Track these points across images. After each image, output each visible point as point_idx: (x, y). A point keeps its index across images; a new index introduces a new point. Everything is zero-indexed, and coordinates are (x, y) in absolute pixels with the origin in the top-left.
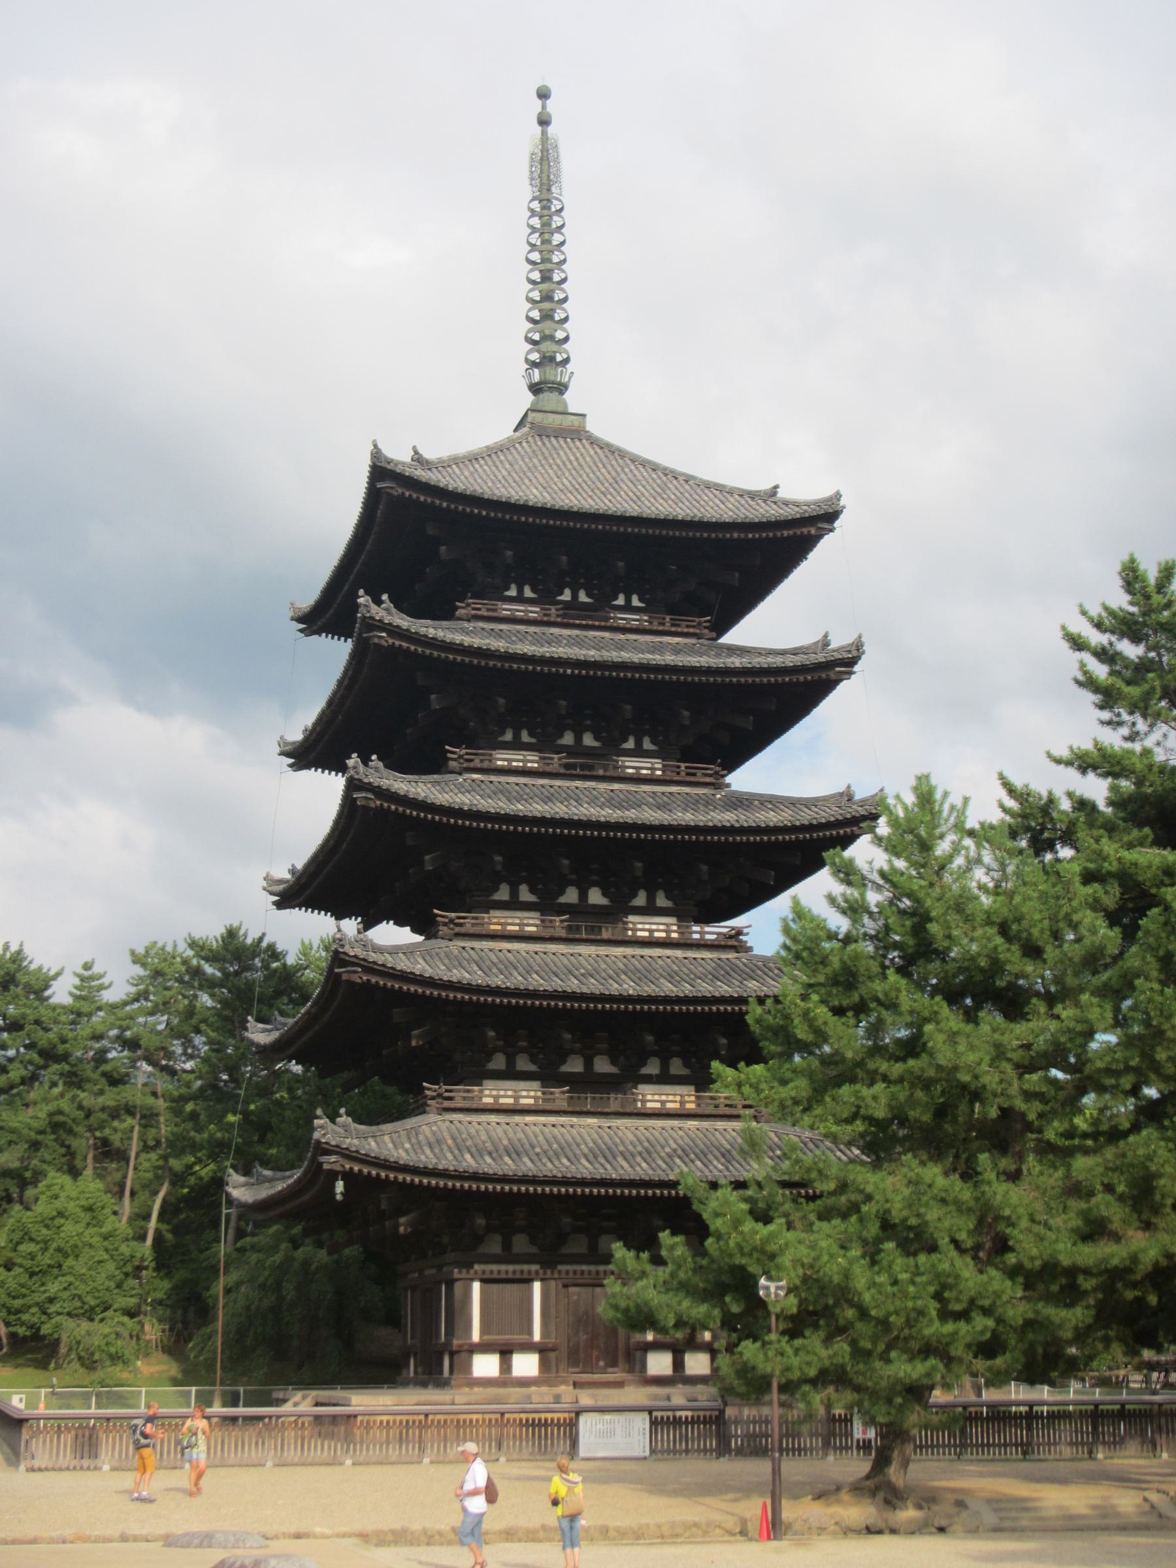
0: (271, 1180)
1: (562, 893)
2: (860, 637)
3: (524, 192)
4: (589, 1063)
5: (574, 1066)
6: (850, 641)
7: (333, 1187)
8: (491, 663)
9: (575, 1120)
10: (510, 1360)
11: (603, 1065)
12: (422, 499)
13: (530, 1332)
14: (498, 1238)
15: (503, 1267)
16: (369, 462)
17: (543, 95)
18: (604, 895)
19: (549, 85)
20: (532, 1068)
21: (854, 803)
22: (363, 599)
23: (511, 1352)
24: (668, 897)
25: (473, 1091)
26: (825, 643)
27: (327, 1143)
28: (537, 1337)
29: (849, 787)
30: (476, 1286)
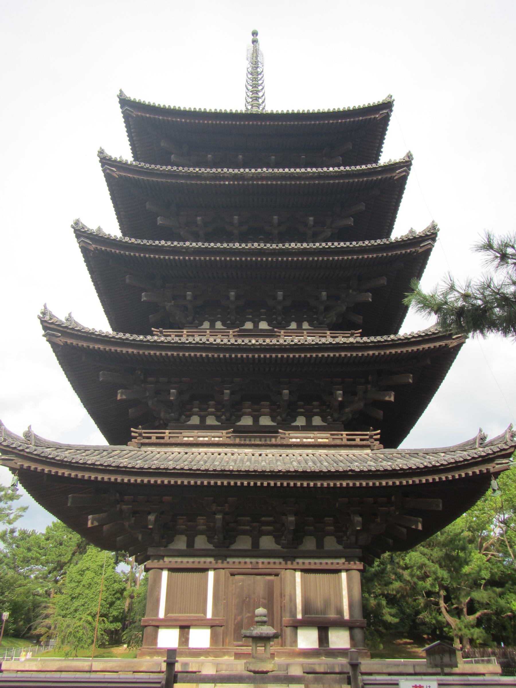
1: (244, 325)
2: (410, 152)
3: (245, 65)
4: (256, 420)
5: (247, 421)
9: (235, 450)
10: (188, 633)
11: (265, 421)
13: (205, 612)
14: (184, 538)
15: (185, 560)
16: (118, 100)
17: (255, 34)
18: (269, 325)
19: (257, 30)
20: (217, 423)
23: (188, 627)
24: (309, 325)
25: (164, 433)
30: (165, 574)
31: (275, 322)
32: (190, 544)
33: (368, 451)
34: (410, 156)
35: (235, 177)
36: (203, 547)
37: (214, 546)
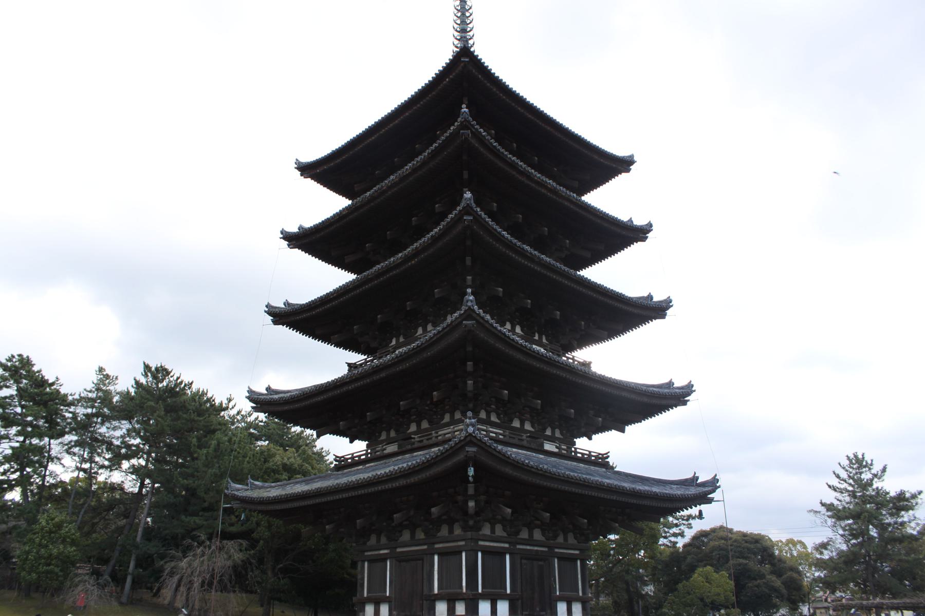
0: (261, 488)
4: (522, 424)
5: (516, 424)
6: (646, 223)
7: (467, 472)
8: (514, 173)
11: (528, 427)
12: (480, 76)
18: (522, 330)
20: (497, 421)
21: (654, 302)
22: (465, 109)
26: (631, 220)
27: (475, 437)
28: (508, 591)
29: (650, 293)
30: (480, 554)
31: (525, 329)
32: (493, 531)
33: (604, 470)
34: (650, 225)
35: (554, 191)
36: (500, 535)
37: (508, 534)
